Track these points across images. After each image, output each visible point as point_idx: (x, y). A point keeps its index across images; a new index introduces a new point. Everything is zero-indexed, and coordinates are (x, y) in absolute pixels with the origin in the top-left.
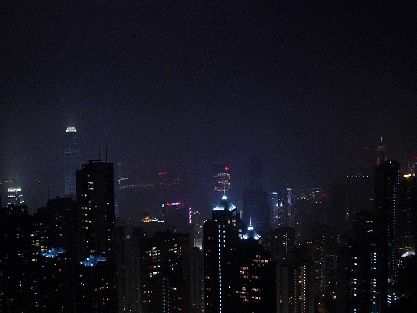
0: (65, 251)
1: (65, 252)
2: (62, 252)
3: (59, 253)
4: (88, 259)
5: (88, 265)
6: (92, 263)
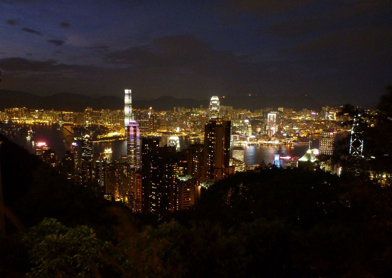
2: (191, 178)
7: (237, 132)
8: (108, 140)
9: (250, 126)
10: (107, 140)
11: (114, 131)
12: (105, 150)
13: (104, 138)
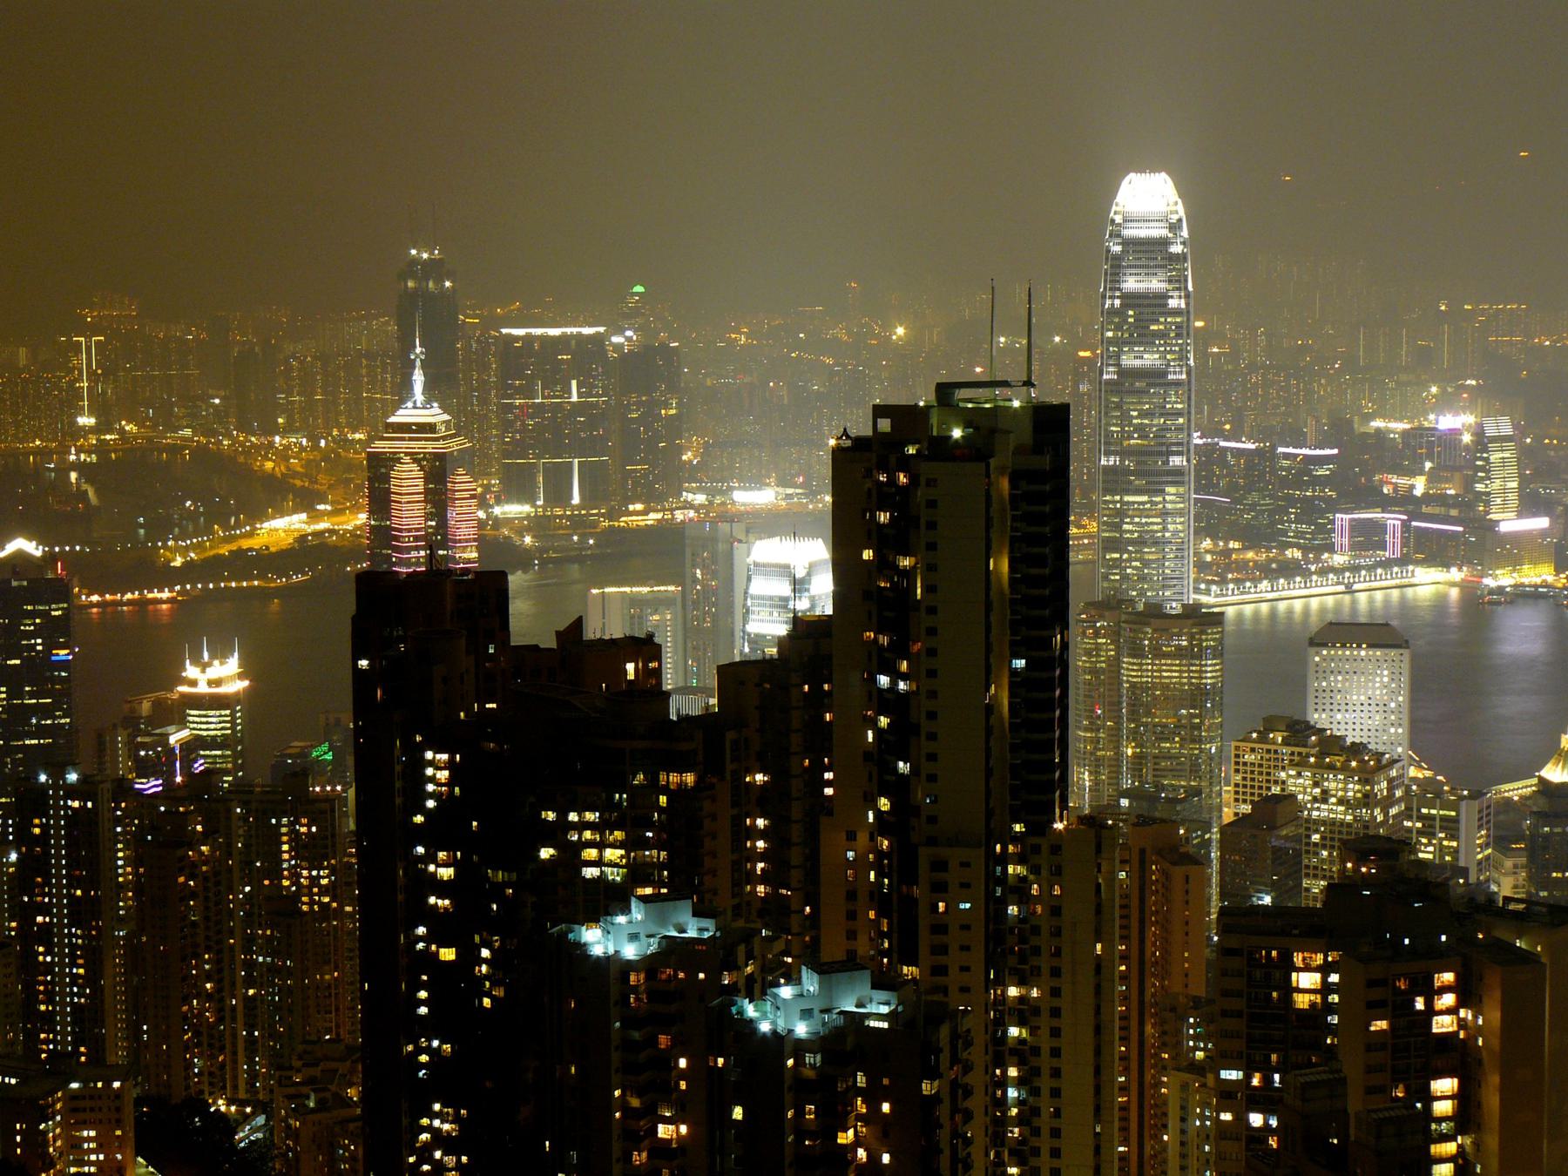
0: (707, 930)
1: (706, 935)
2: (692, 933)
3: (665, 937)
4: (786, 992)
5: (781, 1026)
6: (806, 1014)
7: (1392, 483)
8: (251, 578)
9: (1505, 426)
10: (239, 580)
11: (306, 501)
12: (191, 671)
13: (218, 557)
